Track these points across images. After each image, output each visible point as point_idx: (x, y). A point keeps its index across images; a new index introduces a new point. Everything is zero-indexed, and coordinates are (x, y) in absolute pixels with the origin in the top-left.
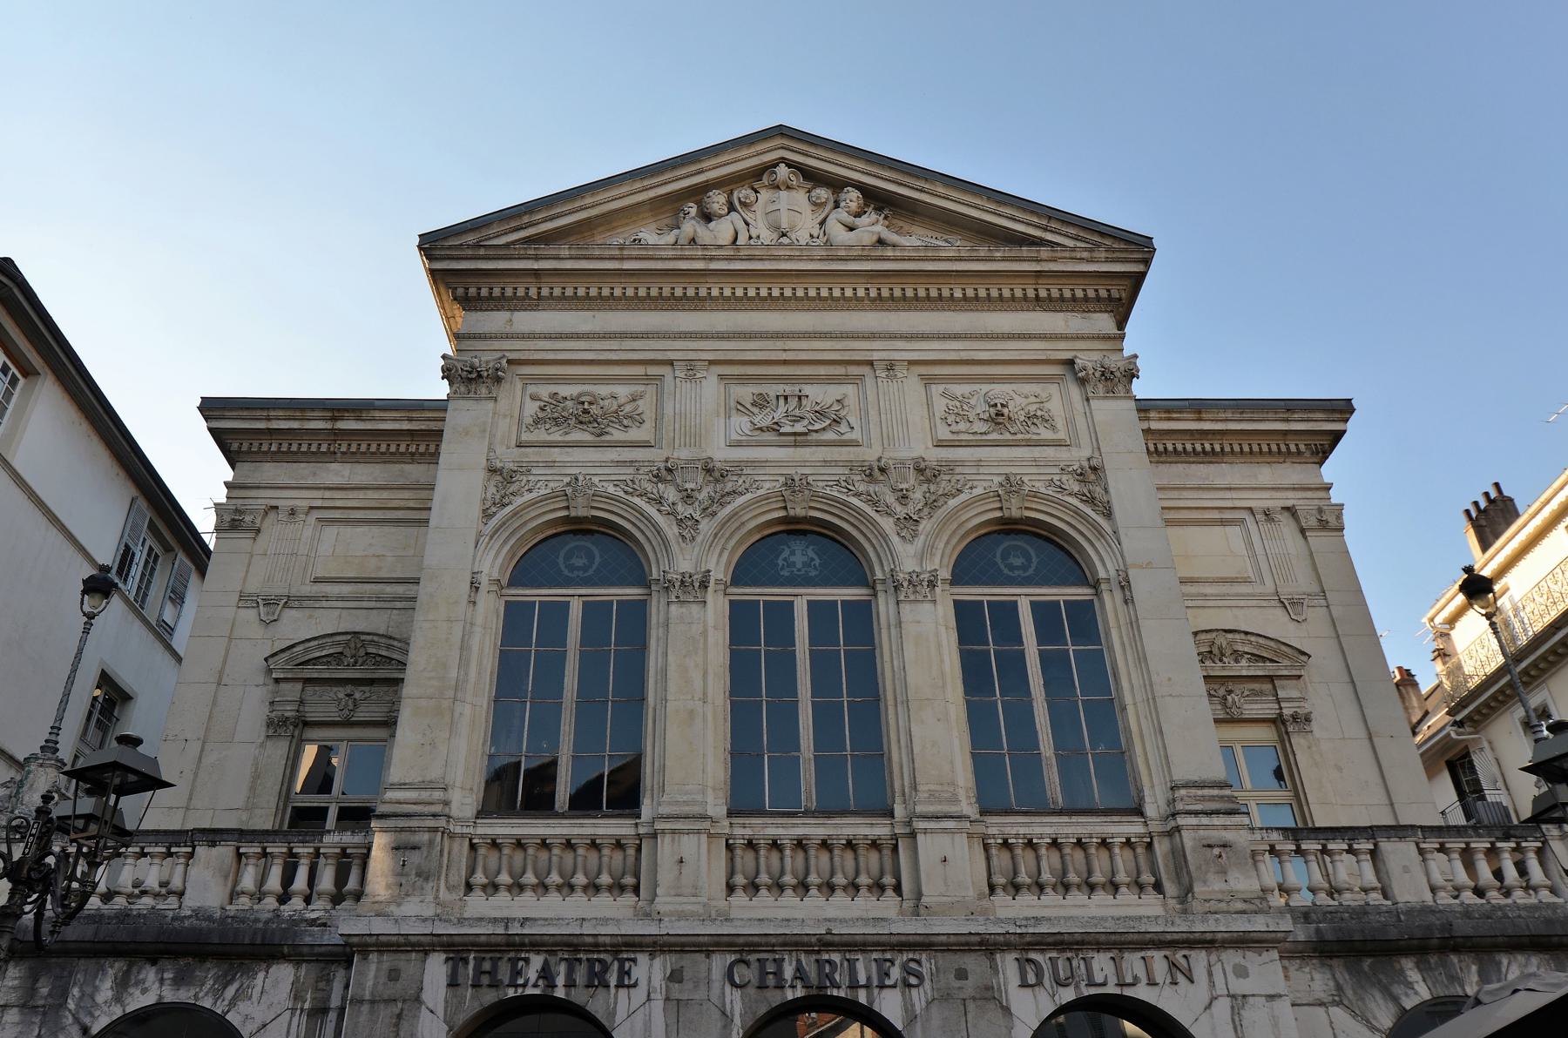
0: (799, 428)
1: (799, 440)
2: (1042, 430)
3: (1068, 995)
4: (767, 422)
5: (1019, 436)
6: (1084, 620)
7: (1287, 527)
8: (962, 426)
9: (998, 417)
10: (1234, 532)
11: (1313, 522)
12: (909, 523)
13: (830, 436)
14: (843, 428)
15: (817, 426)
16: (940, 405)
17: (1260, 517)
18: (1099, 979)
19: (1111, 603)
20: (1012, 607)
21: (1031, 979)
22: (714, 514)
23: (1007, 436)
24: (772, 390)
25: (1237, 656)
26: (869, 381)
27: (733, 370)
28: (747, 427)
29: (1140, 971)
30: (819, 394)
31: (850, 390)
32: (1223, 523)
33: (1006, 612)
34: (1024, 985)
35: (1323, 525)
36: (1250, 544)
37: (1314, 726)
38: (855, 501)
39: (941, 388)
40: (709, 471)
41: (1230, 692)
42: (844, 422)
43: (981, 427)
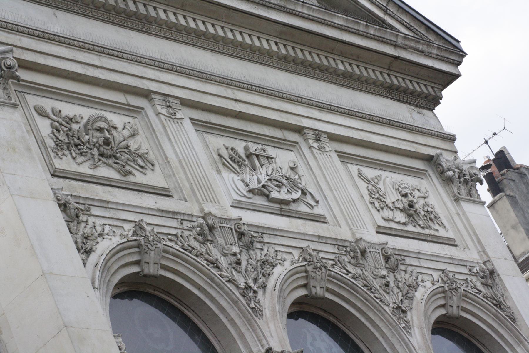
0: (283, 195)
1: (283, 208)
2: (437, 227)
4: (254, 185)
5: (427, 231)
8: (387, 213)
9: (410, 210)
13: (303, 208)
22: (264, 287)
23: (418, 230)
24: (240, 146)
27: (211, 119)
28: (243, 189)
30: (284, 159)
40: (241, 235)
43: (402, 218)
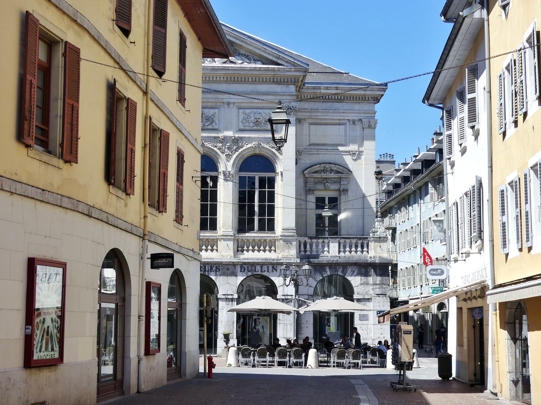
3: (250, 274)
6: (271, 182)
7: (358, 127)
10: (342, 127)
11: (367, 126)
12: (228, 156)
13: (210, 127)
14: (214, 124)
15: (207, 124)
16: (242, 116)
17: (351, 123)
18: (257, 270)
19: (278, 179)
20: (254, 178)
21: (243, 270)
25: (331, 171)
26: (222, 108)
29: (266, 270)
31: (216, 111)
32: (339, 124)
33: (252, 180)
34: (241, 271)
35: (370, 127)
36: (346, 132)
37: (349, 193)
38: (215, 149)
39: (242, 110)
41: (327, 182)
42: (214, 123)
